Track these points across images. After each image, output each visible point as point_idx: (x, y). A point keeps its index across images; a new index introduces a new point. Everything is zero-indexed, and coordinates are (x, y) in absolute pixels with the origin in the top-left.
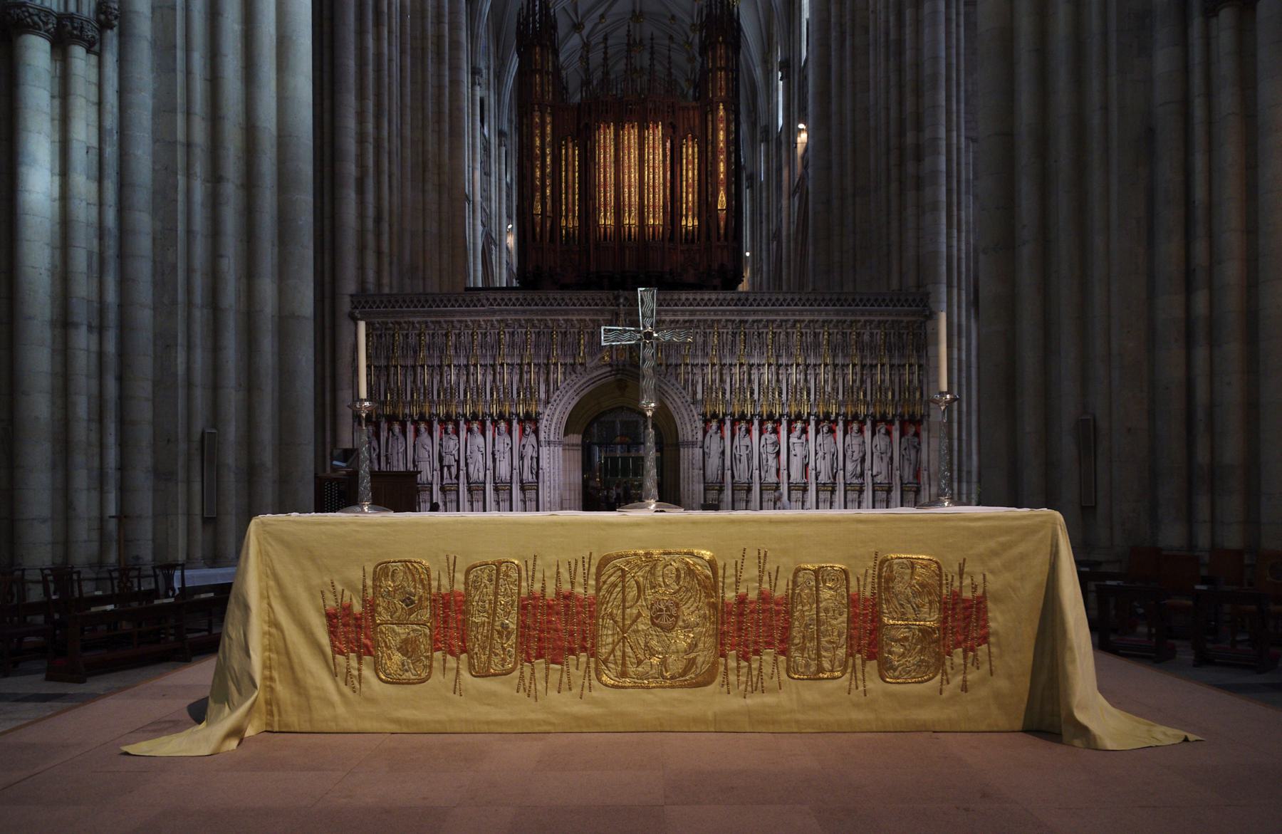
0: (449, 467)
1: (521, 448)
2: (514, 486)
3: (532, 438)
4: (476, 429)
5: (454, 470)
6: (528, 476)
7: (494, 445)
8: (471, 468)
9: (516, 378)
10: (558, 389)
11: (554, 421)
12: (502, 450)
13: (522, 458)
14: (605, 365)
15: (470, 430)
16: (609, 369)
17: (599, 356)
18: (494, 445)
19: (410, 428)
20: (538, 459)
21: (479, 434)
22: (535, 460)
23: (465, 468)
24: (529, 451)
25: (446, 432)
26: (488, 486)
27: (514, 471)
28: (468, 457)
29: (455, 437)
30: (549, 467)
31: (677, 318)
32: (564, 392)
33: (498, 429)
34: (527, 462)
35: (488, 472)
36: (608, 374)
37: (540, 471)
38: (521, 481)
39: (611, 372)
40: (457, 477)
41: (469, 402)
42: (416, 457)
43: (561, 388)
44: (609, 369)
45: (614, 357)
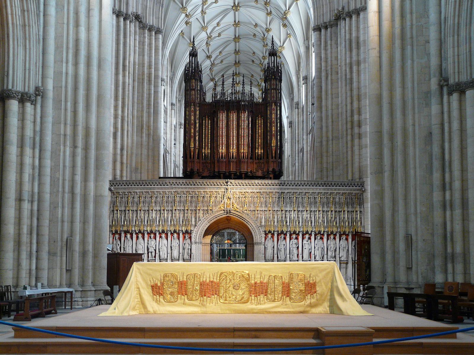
0: (151, 252)
1: (184, 245)
3: (189, 241)
5: (153, 254)
7: (171, 243)
8: (161, 253)
9: (182, 216)
12: (175, 246)
13: (184, 249)
15: (161, 237)
17: (219, 207)
18: (171, 243)
19: (134, 236)
20: (191, 249)
21: (165, 239)
22: (190, 250)
23: (158, 253)
24: (187, 246)
25: (150, 238)
28: (160, 248)
29: (154, 240)
31: (253, 191)
34: (186, 251)
35: (168, 254)
37: (192, 255)
39: (224, 213)
40: (155, 257)
44: (224, 212)
45: (225, 207)
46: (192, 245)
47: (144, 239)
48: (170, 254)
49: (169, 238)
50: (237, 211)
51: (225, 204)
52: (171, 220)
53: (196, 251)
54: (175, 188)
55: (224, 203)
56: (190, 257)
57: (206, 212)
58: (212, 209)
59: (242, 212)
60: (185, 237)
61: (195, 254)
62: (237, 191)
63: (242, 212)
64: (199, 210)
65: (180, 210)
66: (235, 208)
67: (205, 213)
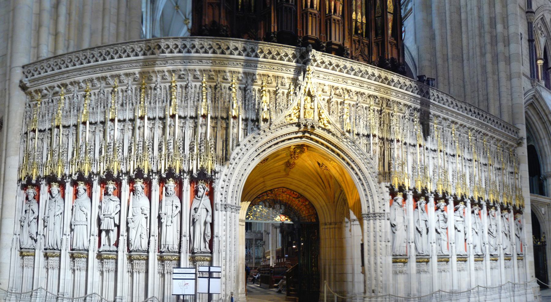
0: (108, 232)
1: (193, 211)
2: (183, 256)
3: (206, 201)
4: (140, 189)
5: (113, 235)
6: (200, 245)
7: (160, 208)
9: (189, 133)
11: (233, 182)
12: (169, 213)
13: (193, 222)
14: (292, 124)
15: (133, 191)
17: (287, 113)
18: (160, 208)
19: (69, 190)
20: (212, 225)
21: (144, 195)
22: (209, 226)
23: (126, 234)
24: (203, 216)
25: (106, 193)
26: (151, 255)
27: (184, 239)
28: (130, 220)
29: (116, 198)
30: (226, 235)
33: (166, 189)
34: (199, 228)
35: (152, 238)
36: (294, 136)
37: (215, 239)
38: (192, 252)
39: (296, 133)
40: (117, 244)
41: (133, 157)
42: (73, 220)
43: (242, 144)
44: (296, 129)
45: (302, 116)
46: (216, 213)
47: (90, 196)
48: (157, 238)
49: (153, 193)
50: (329, 131)
52: (160, 145)
53: (225, 231)
54: (174, 58)
55: (299, 105)
56: (211, 246)
57: (250, 124)
58: (268, 117)
60: (196, 192)
61: (224, 238)
65: (185, 118)
67: (249, 128)
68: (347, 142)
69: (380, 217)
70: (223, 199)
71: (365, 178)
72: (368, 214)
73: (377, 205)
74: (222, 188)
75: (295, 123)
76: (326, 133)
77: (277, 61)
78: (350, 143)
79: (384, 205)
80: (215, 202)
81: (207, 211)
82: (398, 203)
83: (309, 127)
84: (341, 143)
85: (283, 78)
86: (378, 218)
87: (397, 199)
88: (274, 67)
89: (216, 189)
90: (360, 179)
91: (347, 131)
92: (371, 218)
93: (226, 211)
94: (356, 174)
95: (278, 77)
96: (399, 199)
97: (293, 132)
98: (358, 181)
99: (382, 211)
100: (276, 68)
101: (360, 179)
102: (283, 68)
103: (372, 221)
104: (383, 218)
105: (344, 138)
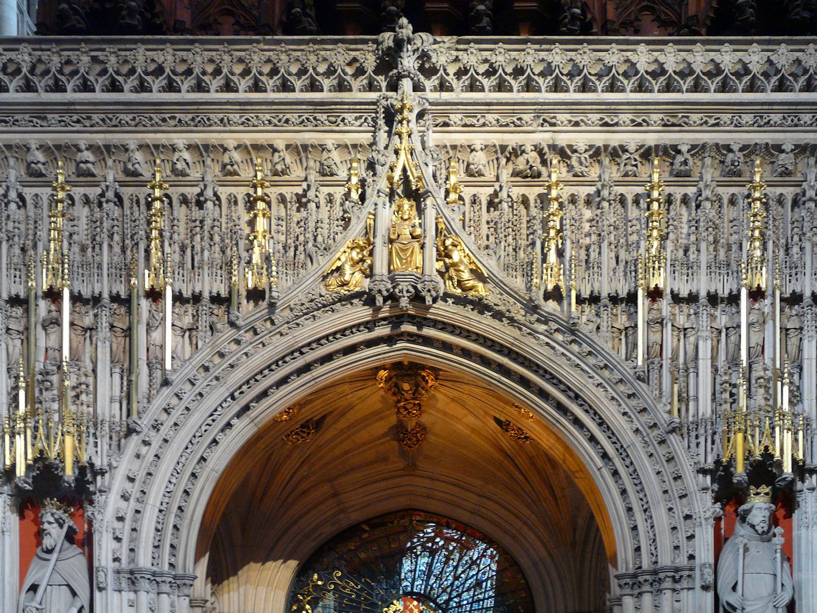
10: (166, 383)
16: (361, 313)
17: (325, 264)
31: (614, 139)
32: (189, 393)
44: (361, 313)
45: (381, 268)
50: (481, 306)
51: (379, 242)
55: (369, 232)
59: (518, 312)
62: (478, 139)
63: (518, 312)
64: (155, 295)
66: (466, 275)
68: (548, 334)
69: (675, 581)
70: (124, 556)
71: (622, 451)
72: (635, 576)
73: (665, 541)
74: (121, 519)
75: (358, 295)
76: (474, 315)
77: (297, 95)
78: (560, 337)
79: (691, 537)
80: (96, 564)
81: (74, 594)
82: (753, 526)
83: (404, 302)
84: (530, 341)
85: (323, 148)
86: (668, 584)
87: (748, 512)
88: (288, 116)
89: (96, 525)
90: (605, 456)
91: (547, 296)
92: (646, 587)
93: (136, 592)
94: (592, 439)
95: (305, 147)
96: (754, 512)
97: (359, 325)
98: (600, 463)
99: (682, 561)
100: (293, 117)
101: (605, 456)
102: (318, 116)
103: (647, 599)
104: (685, 584)
105: (538, 320)
